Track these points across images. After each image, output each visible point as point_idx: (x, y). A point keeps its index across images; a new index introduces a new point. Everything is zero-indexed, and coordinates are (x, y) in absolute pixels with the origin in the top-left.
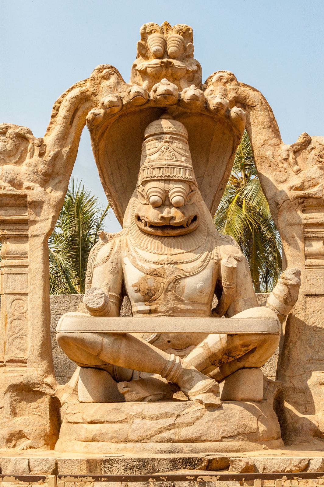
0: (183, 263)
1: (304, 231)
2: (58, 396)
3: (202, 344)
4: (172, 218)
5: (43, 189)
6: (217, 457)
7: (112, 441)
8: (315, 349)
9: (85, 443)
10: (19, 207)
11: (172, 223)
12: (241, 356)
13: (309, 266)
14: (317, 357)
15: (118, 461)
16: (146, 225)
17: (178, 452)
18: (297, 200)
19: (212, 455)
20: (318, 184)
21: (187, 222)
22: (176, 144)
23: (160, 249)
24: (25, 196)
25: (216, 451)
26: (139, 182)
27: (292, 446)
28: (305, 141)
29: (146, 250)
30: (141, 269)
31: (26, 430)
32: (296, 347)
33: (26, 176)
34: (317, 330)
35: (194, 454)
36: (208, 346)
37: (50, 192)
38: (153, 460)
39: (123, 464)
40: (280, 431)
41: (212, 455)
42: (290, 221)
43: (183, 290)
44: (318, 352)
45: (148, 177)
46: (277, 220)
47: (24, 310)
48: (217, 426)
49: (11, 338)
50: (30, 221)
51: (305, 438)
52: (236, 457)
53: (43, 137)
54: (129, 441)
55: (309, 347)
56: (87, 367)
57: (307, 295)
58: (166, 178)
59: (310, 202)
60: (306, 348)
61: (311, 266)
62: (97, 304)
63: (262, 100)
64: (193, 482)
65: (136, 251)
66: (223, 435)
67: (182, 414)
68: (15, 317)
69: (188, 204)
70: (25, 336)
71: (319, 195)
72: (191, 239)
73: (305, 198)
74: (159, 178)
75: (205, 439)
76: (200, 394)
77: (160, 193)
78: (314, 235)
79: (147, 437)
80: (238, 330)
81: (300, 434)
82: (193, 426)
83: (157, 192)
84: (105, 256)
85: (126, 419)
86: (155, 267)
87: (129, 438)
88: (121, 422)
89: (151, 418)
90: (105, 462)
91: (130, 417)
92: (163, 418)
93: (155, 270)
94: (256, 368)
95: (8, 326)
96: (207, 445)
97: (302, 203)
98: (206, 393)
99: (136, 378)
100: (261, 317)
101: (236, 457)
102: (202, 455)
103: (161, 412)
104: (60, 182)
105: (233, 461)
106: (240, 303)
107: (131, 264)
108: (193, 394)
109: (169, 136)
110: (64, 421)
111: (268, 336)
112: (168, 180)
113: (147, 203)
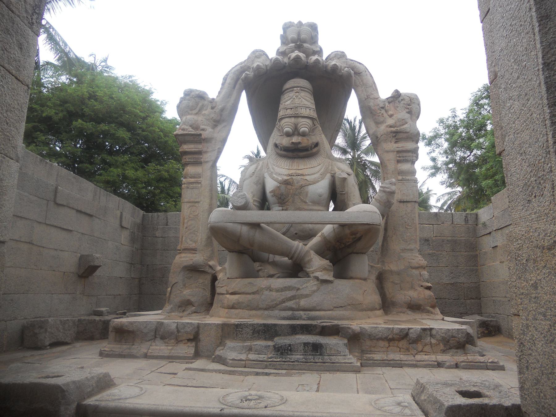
0: (308, 175)
1: (397, 156)
2: (217, 275)
3: (320, 234)
4: (299, 143)
5: (212, 130)
6: (329, 324)
7: (246, 309)
8: (407, 242)
9: (226, 310)
10: (197, 143)
11: (300, 146)
12: (350, 243)
13: (401, 180)
14: (408, 247)
15: (247, 325)
16: (281, 150)
17: (298, 319)
18: (391, 134)
19: (325, 322)
20: (407, 123)
21: (311, 146)
22: (303, 94)
23: (291, 166)
24: (200, 135)
25: (329, 318)
26: (278, 121)
27: (390, 315)
28: (397, 95)
29: (281, 167)
30: (276, 180)
31: (193, 299)
32: (392, 240)
33: (202, 122)
34: (408, 227)
35: (311, 321)
36: (324, 235)
37: (218, 133)
38: (275, 325)
39: (251, 328)
40: (381, 303)
41: (325, 322)
42: (386, 149)
43: (307, 195)
44: (409, 244)
45: (283, 115)
46: (377, 149)
47: (197, 214)
48: (331, 298)
49: (187, 233)
50: (203, 152)
51: (400, 310)
52: (345, 325)
53: (215, 97)
54: (260, 309)
55: (402, 240)
56: (233, 252)
57: (400, 202)
58: (295, 115)
59: (401, 136)
60: (400, 241)
61: (403, 180)
62: (240, 203)
63: (366, 70)
64: (307, 347)
65: (273, 169)
66: (335, 306)
67: (301, 288)
68: (190, 219)
69: (312, 134)
70: (197, 232)
71: (408, 130)
72: (314, 159)
73: (396, 132)
74: (290, 115)
75: (320, 308)
76: (317, 272)
77: (291, 126)
78: (404, 159)
79: (273, 306)
80: (347, 221)
81: (397, 307)
82: (310, 298)
83: (288, 125)
84: (252, 173)
85: (257, 291)
86: (286, 178)
87: (259, 306)
88: (254, 293)
89: (277, 291)
90: (237, 326)
91: (261, 290)
92: (286, 290)
93: (286, 180)
94: (362, 253)
95: (185, 225)
96: (322, 313)
97: (395, 136)
98: (321, 271)
99: (271, 260)
100: (366, 211)
101: (345, 325)
102: (317, 322)
103: (285, 286)
104: (225, 126)
105: (344, 327)
106: (350, 206)
107: (269, 177)
108: (311, 272)
109: (299, 88)
110: (216, 293)
111: (371, 226)
112: (296, 117)
113: (283, 134)
